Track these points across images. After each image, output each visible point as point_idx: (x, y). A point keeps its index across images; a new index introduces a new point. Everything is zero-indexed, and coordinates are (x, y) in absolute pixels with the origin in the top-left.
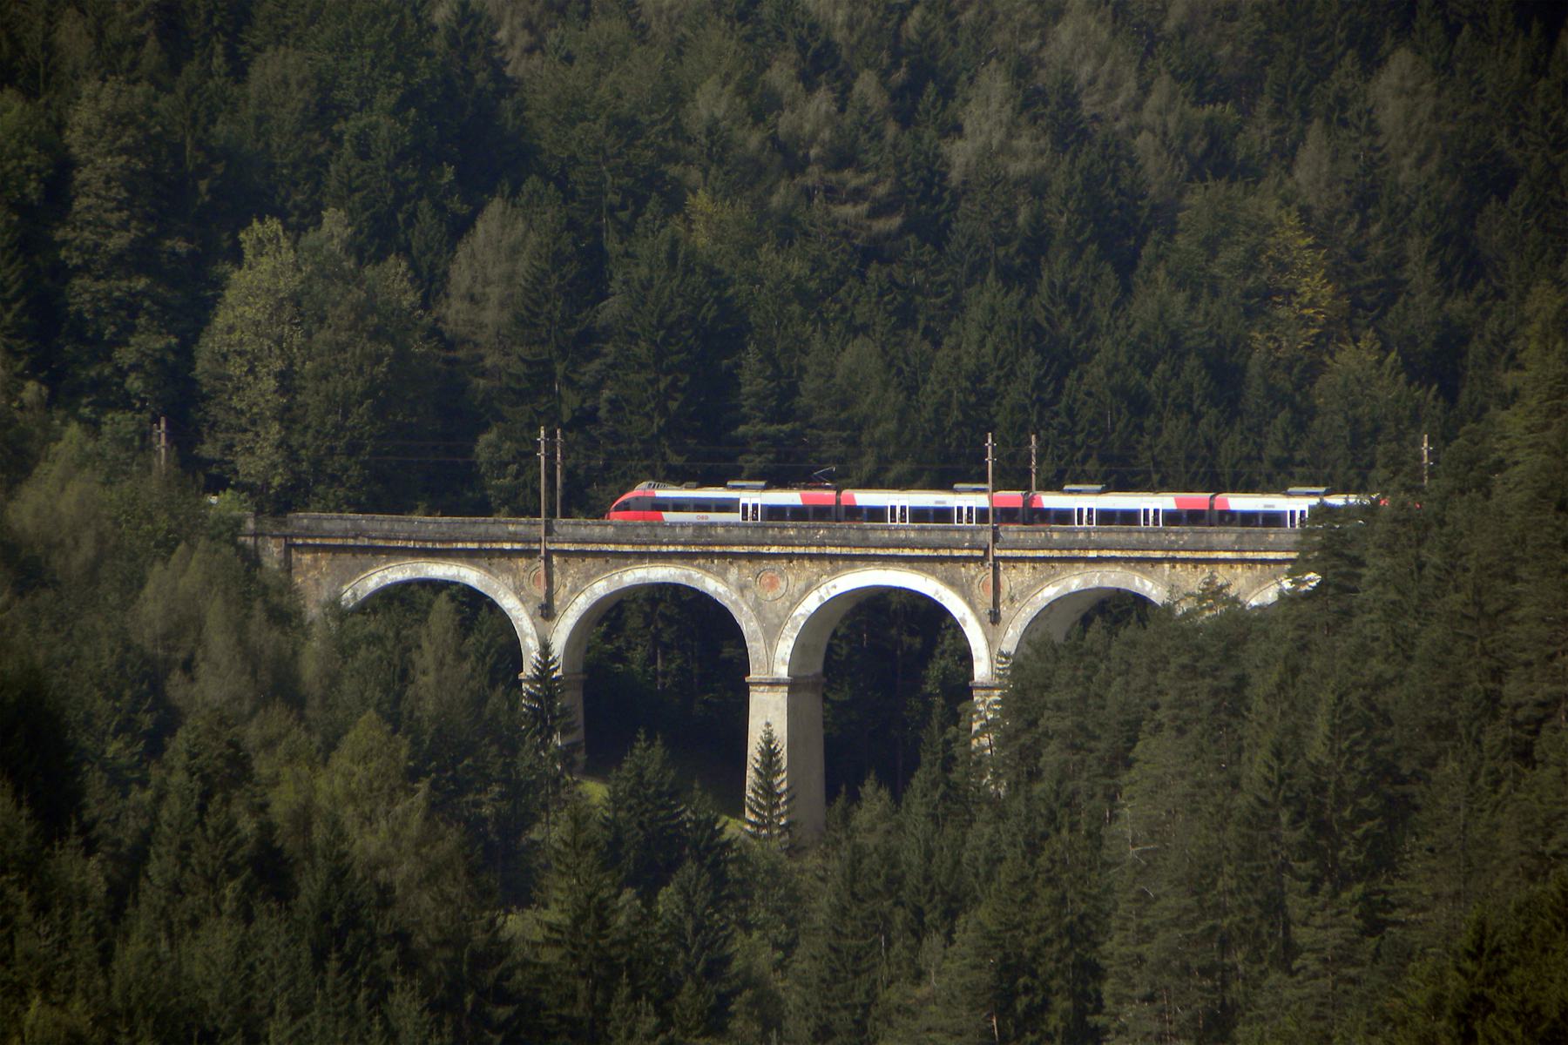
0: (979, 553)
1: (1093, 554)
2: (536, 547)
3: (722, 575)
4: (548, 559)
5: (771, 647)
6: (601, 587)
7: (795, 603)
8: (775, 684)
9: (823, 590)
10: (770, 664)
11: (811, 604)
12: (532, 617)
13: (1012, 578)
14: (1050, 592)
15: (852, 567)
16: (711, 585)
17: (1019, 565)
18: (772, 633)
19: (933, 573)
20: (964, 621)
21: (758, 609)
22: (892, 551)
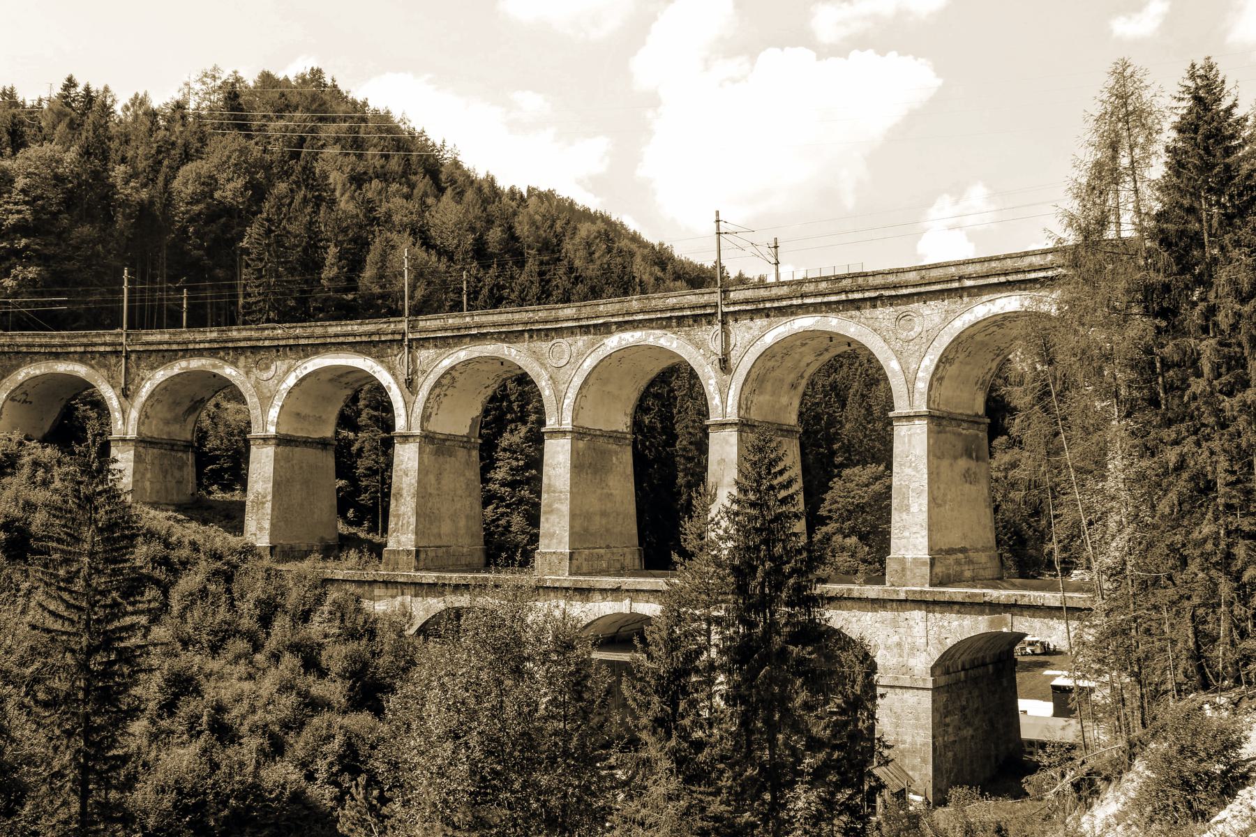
0: (398, 337)
1: (474, 332)
2: (119, 348)
3: (234, 364)
4: (127, 358)
5: (265, 412)
6: (161, 375)
7: (281, 381)
8: (265, 440)
9: (298, 371)
10: (264, 428)
11: (291, 381)
12: (118, 398)
13: (424, 355)
14: (447, 363)
15: (316, 353)
16: (229, 371)
17: (426, 344)
18: (266, 401)
19: (369, 354)
20: (390, 388)
21: (257, 386)
22: (341, 339)
